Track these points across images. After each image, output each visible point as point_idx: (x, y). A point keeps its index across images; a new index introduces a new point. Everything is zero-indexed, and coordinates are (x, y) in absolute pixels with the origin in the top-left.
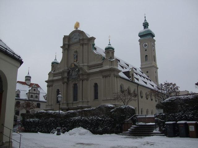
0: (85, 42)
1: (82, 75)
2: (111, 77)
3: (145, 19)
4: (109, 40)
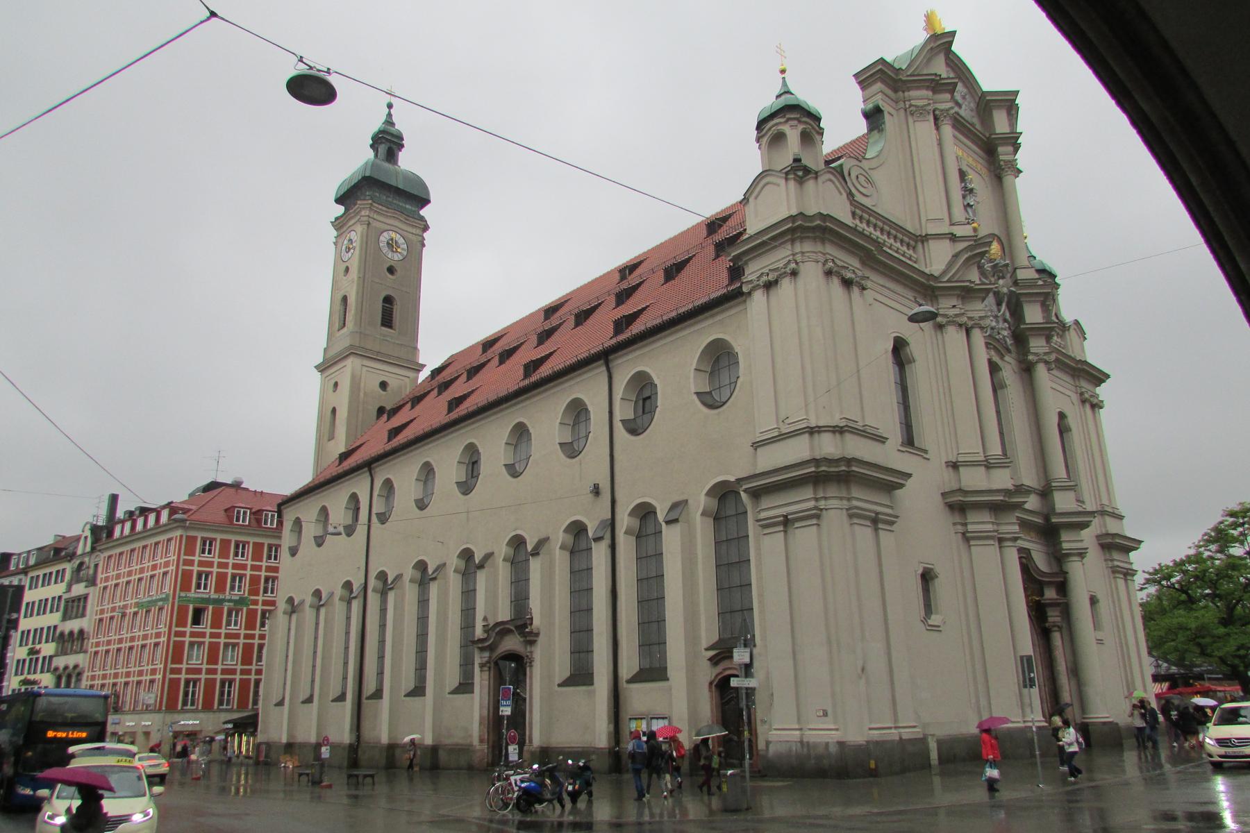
2: (801, 280)
4: (783, 72)
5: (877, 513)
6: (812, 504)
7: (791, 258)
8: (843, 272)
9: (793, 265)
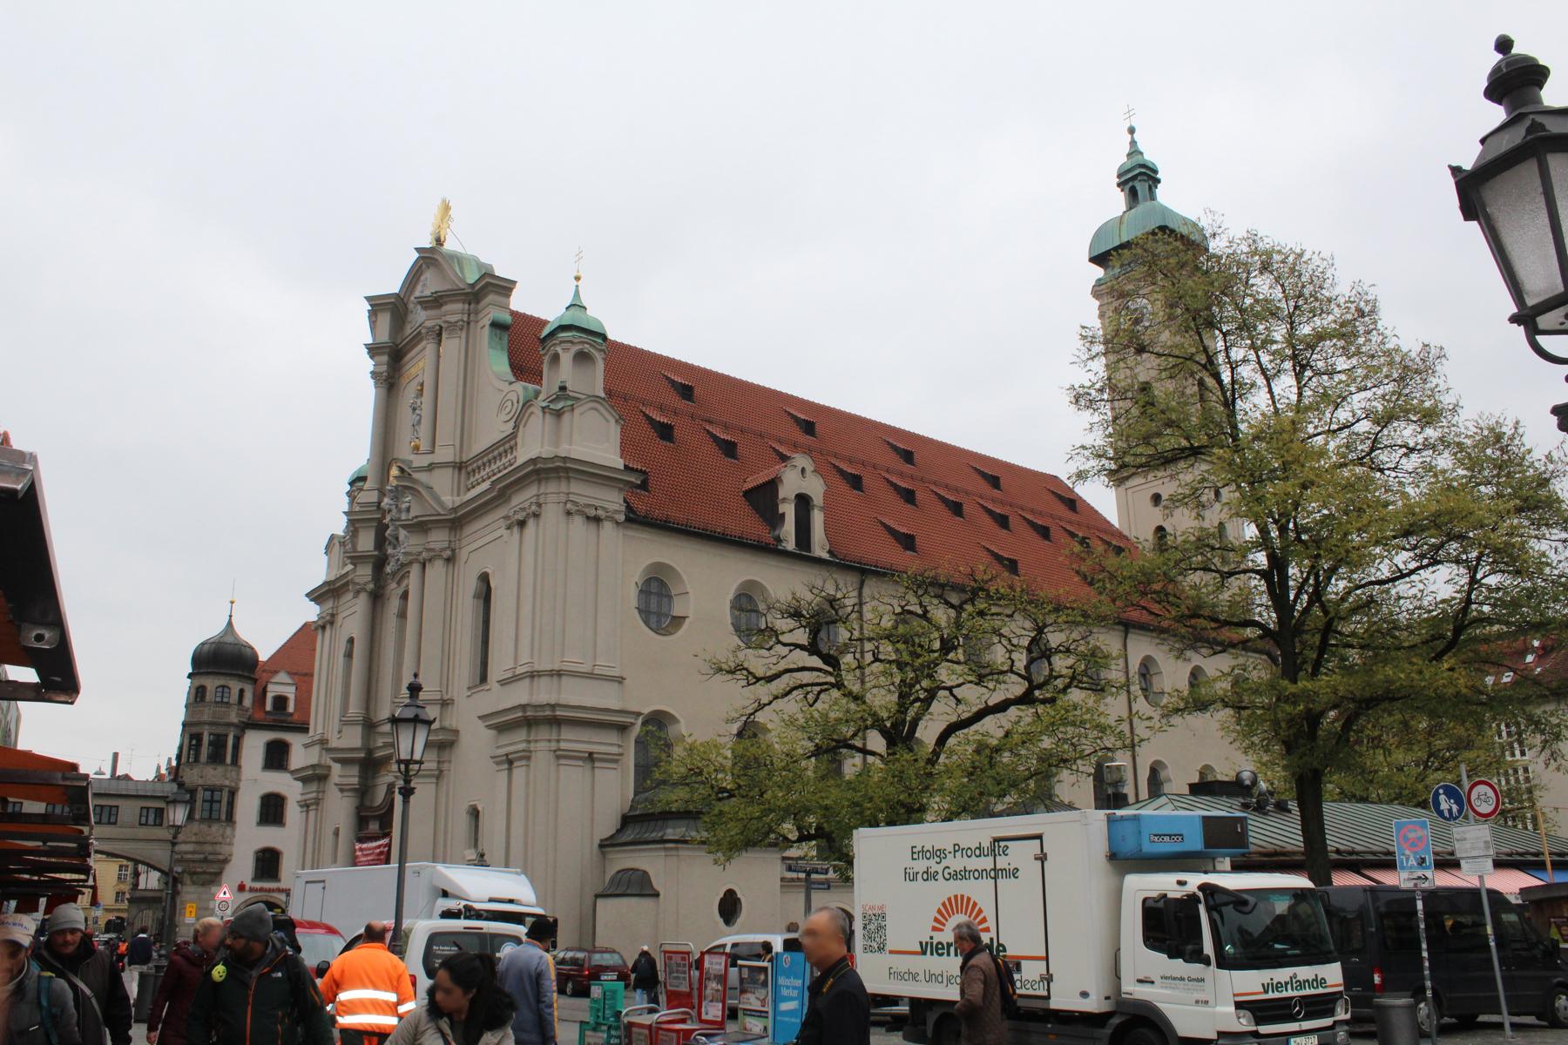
0: (449, 318)
1: (421, 527)
3: (1133, 143)
4: (578, 278)
5: (591, 754)
6: (523, 746)
7: (534, 500)
8: (587, 510)
9: (534, 508)
